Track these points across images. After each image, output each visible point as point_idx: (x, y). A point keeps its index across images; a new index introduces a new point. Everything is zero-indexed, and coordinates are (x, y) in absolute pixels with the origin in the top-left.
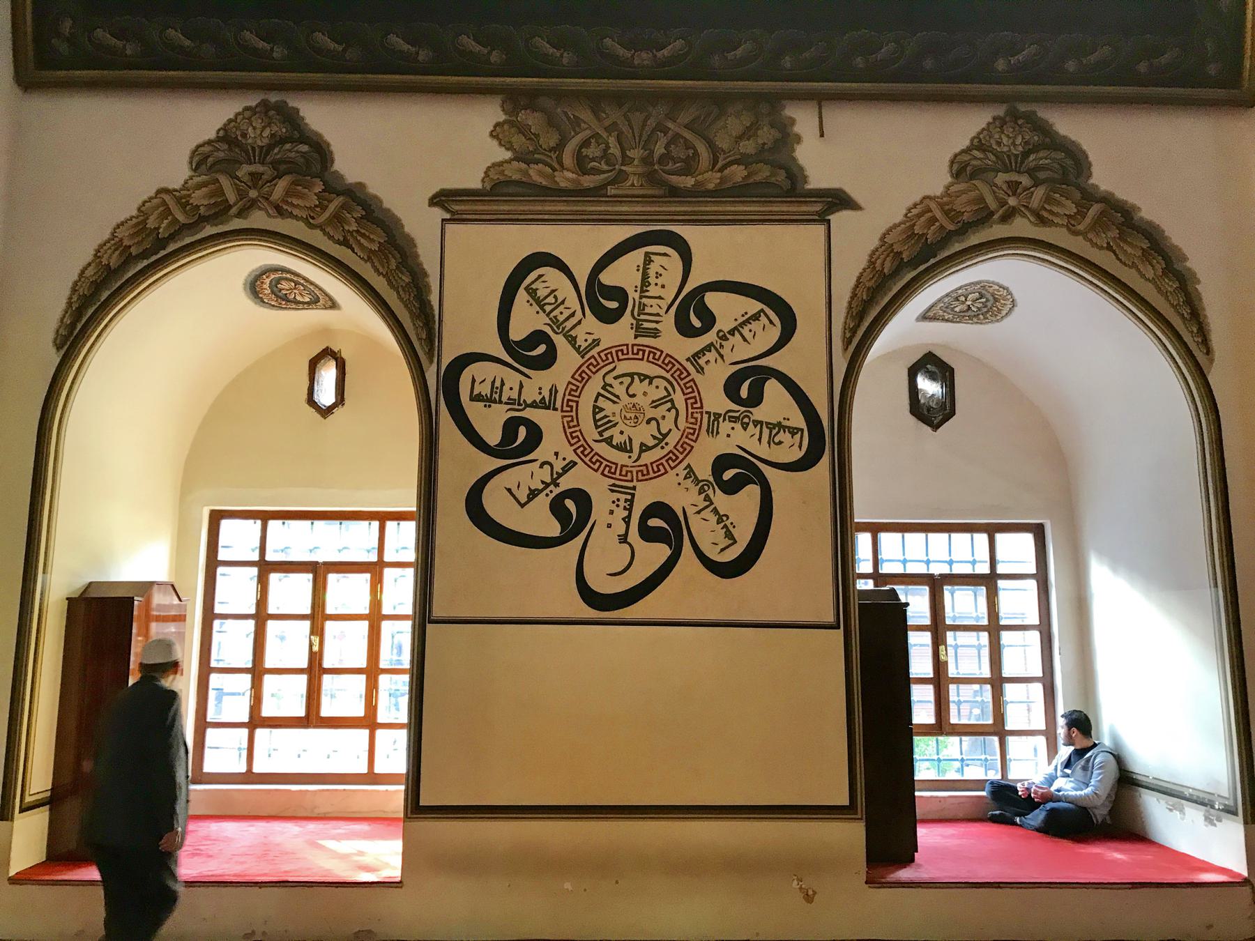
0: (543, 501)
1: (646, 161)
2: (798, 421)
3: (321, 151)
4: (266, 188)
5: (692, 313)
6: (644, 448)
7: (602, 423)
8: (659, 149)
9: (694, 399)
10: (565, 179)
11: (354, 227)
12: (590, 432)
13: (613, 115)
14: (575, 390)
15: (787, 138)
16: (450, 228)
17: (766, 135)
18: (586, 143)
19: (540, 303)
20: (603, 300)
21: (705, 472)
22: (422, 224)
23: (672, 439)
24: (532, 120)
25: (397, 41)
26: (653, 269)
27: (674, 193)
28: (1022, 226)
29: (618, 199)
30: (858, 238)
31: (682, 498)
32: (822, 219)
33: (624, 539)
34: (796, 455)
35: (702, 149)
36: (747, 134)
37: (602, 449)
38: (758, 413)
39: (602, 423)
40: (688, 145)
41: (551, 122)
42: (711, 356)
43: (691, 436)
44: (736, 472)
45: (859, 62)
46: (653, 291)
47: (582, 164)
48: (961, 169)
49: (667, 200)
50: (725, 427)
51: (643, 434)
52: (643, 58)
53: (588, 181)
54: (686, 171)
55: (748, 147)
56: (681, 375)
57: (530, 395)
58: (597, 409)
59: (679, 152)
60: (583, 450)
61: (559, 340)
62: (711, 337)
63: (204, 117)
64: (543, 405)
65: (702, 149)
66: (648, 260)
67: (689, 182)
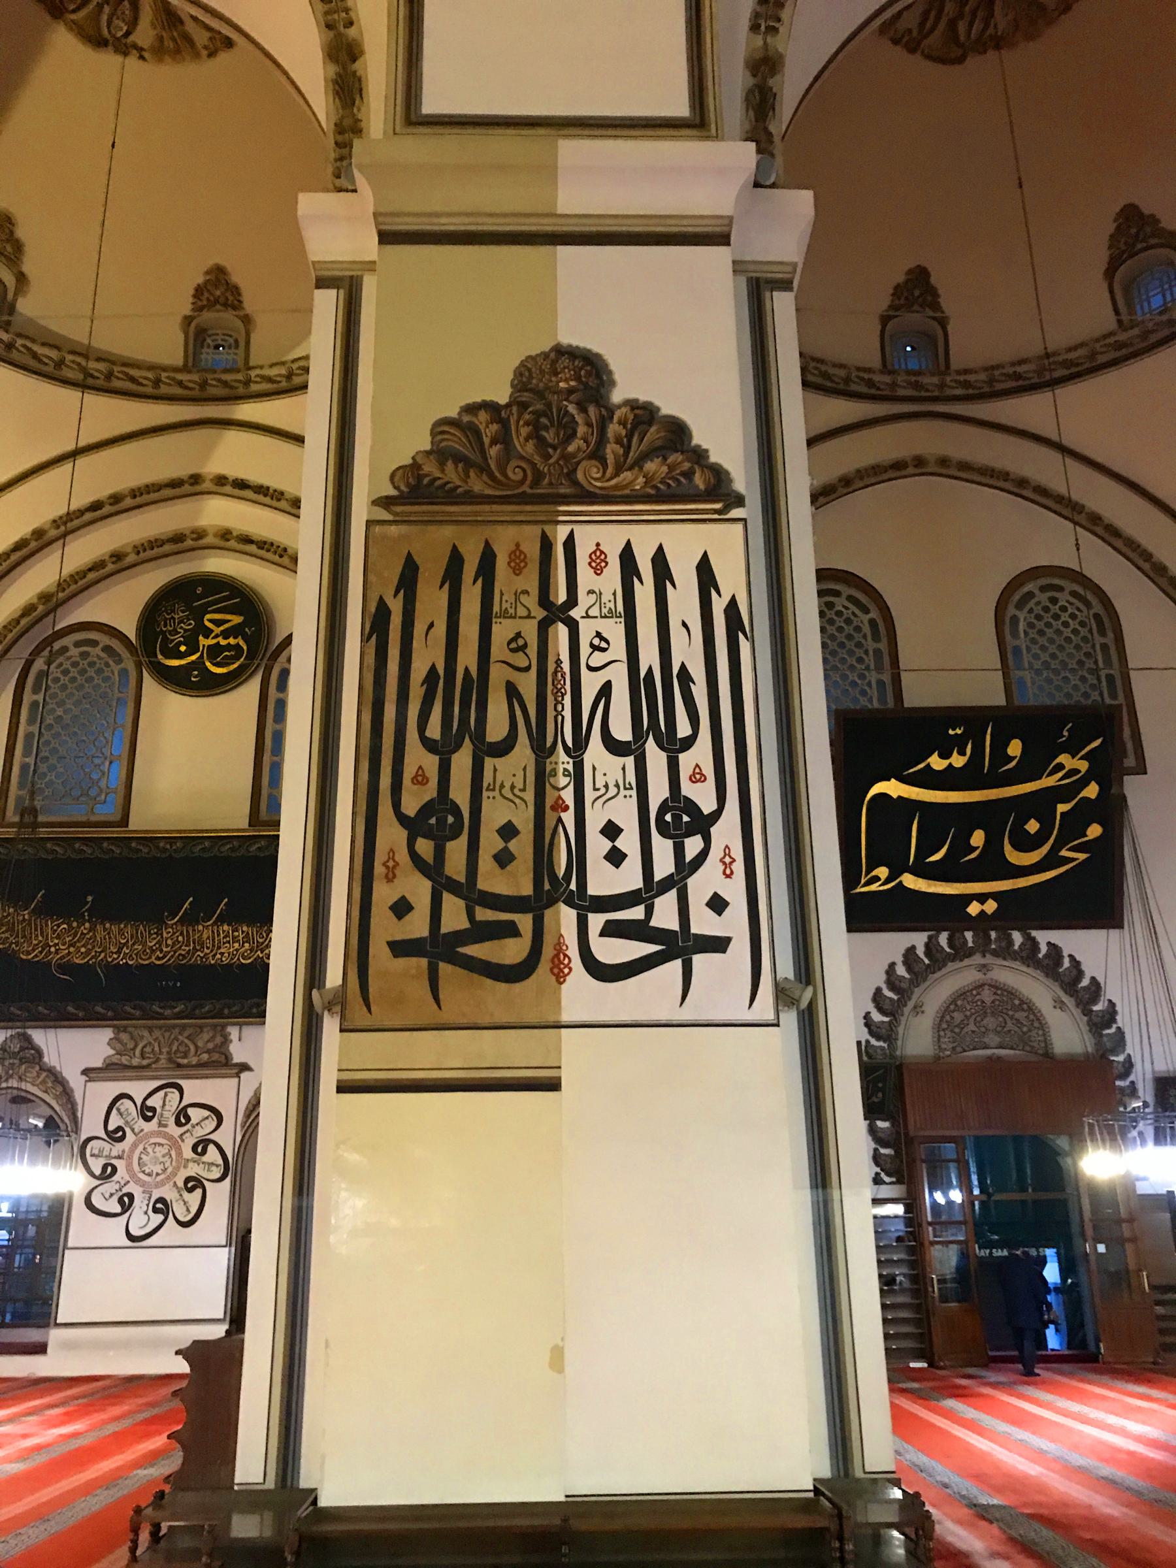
0: (116, 1198)
1: (168, 1053)
2: (221, 1162)
3: (39, 1053)
5: (182, 1117)
6: (158, 1174)
8: (174, 1048)
9: (180, 1153)
10: (136, 1061)
11: (50, 1085)
12: (136, 1167)
13: (157, 1033)
15: (226, 1041)
16: (89, 1084)
17: (219, 1040)
18: (145, 1047)
19: (121, 1114)
20: (147, 1112)
21: (181, 1184)
23: (169, 1170)
24: (124, 1037)
25: (70, 1009)
26: (168, 1099)
27: (179, 1066)
29: (157, 1069)
33: (146, 1213)
34: (218, 1175)
35: (192, 1048)
36: (213, 1038)
37: (141, 1176)
38: (205, 1158)
40: (186, 1046)
41: (132, 1038)
42: (188, 1135)
43: (177, 1169)
44: (194, 1184)
45: (254, 1010)
46: (167, 1108)
47: (143, 1057)
49: (177, 1068)
50: (191, 1164)
51: (157, 1169)
52: (168, 1012)
53: (145, 1062)
54: (185, 1057)
55: (210, 1046)
56: (175, 1144)
57: (114, 1153)
58: (140, 1159)
59: (182, 1049)
60: (133, 1175)
61: (128, 1130)
62: (188, 1126)
64: (119, 1157)
66: (166, 1095)
67: (185, 1061)
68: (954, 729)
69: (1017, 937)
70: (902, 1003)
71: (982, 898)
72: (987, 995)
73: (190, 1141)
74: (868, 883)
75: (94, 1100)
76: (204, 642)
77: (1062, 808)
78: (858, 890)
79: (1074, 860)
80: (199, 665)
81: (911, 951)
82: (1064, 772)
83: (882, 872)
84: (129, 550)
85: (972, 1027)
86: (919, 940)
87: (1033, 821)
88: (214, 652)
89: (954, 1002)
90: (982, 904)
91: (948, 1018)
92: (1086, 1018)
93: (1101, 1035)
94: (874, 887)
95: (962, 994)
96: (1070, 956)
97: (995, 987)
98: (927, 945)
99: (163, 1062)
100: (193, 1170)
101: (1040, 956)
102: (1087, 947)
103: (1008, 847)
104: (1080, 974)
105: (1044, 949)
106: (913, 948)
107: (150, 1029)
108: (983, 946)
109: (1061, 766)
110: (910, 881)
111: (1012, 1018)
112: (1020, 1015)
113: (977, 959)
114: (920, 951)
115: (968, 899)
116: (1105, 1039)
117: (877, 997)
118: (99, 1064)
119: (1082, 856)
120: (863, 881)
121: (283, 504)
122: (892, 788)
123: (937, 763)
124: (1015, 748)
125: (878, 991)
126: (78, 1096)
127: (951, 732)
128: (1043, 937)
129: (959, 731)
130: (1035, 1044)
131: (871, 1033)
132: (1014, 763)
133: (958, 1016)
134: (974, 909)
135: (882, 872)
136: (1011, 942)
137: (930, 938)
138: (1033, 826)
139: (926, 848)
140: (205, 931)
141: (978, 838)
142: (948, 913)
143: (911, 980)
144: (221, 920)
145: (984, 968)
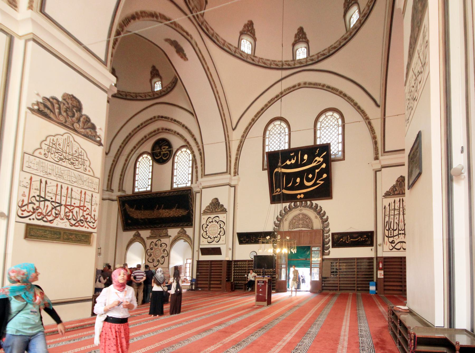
3: (140, 235)
4: (137, 238)
15: (167, 231)
22: (146, 240)
28: (182, 237)
30: (171, 239)
48: (178, 233)
63: (133, 233)
69: (309, 203)
71: (300, 194)
72: (301, 216)
81: (285, 207)
83: (279, 190)
86: (287, 205)
94: (277, 193)
98: (289, 206)
102: (322, 203)
104: (322, 210)
105: (314, 205)
108: (301, 205)
112: (307, 220)
114: (287, 207)
115: (297, 194)
117: (277, 218)
119: (322, 182)
128: (314, 202)
133: (294, 221)
136: (307, 204)
140: (161, 211)
144: (163, 209)
145: (301, 210)
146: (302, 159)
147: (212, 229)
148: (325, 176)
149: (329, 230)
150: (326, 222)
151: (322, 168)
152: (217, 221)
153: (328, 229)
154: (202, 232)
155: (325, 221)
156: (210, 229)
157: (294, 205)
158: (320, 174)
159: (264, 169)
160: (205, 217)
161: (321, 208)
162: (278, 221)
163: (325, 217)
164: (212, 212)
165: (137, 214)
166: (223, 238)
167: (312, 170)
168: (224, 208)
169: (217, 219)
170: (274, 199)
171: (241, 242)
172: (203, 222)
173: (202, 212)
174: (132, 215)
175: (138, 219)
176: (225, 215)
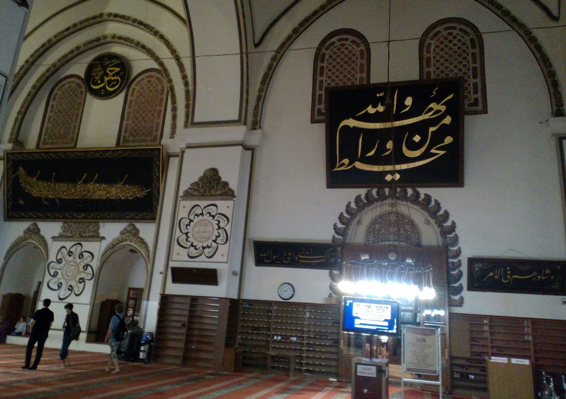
2: (91, 273)
3: (39, 230)
5: (81, 256)
7: (66, 272)
12: (64, 274)
13: (77, 224)
14: (64, 267)
15: (99, 228)
20: (70, 253)
21: (78, 281)
24: (66, 225)
27: (82, 236)
31: (73, 283)
32: (101, 241)
36: (94, 227)
39: (66, 272)
43: (77, 274)
47: (71, 233)
48: (122, 233)
49: (82, 237)
51: (71, 274)
52: (79, 217)
53: (72, 235)
56: (78, 265)
57: (58, 268)
64: (60, 269)
65: (87, 230)
68: (379, 94)
69: (410, 191)
70: (350, 220)
71: (392, 173)
73: (83, 264)
74: (339, 166)
75: (54, 247)
76: (106, 79)
77: (432, 129)
78: (336, 169)
79: (437, 154)
80: (104, 87)
82: (433, 112)
83: (346, 161)
84: (82, 45)
85: (383, 231)
86: (362, 192)
87: (417, 136)
88: (109, 82)
89: (376, 220)
90: (393, 175)
91: (373, 227)
92: (439, 229)
93: (446, 237)
94: (342, 168)
95: (381, 217)
96: (436, 201)
97: (397, 214)
99: (77, 235)
100: (83, 275)
101: (420, 200)
103: (404, 148)
105: (422, 196)
106: (360, 195)
107: (75, 223)
108: (393, 195)
109: (431, 109)
110: (358, 165)
111: (403, 227)
112: (408, 227)
113: (389, 201)
114: (363, 197)
116: (448, 239)
117: (341, 217)
118: (57, 235)
119: (442, 153)
120: (338, 165)
121: (130, 22)
122: (351, 123)
123: (371, 110)
124: (409, 101)
125: (342, 214)
126: (49, 246)
127: (378, 95)
128: (423, 191)
129: (381, 95)
130: (413, 240)
131: (336, 232)
132: (408, 109)
133: (377, 226)
134: (389, 178)
135: (346, 161)
136: (406, 193)
137: (368, 191)
138: (417, 138)
139: (366, 149)
140: (90, 186)
141: (390, 145)
142: (376, 180)
143: (357, 210)
144: (97, 182)
145: (392, 205)
146: (401, 105)
147: (201, 228)
148: (448, 140)
149: (458, 253)
150: (450, 233)
151: (444, 124)
152: (213, 214)
153: (455, 248)
154: (178, 233)
155: (448, 231)
156: (196, 229)
157: (378, 193)
158: (438, 138)
159: (313, 121)
160: (185, 206)
161: (438, 204)
162: (342, 222)
163: (448, 224)
164: (203, 196)
165: (40, 189)
166: (223, 249)
167: (420, 128)
168: (230, 189)
169: (213, 210)
170: (335, 180)
171: (259, 262)
172: (183, 213)
173: (181, 193)
174: (28, 189)
175: (40, 198)
176: (230, 203)
